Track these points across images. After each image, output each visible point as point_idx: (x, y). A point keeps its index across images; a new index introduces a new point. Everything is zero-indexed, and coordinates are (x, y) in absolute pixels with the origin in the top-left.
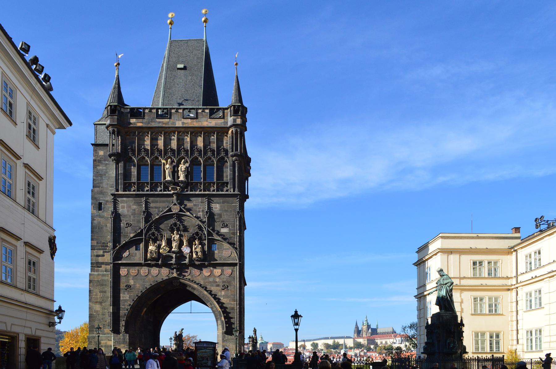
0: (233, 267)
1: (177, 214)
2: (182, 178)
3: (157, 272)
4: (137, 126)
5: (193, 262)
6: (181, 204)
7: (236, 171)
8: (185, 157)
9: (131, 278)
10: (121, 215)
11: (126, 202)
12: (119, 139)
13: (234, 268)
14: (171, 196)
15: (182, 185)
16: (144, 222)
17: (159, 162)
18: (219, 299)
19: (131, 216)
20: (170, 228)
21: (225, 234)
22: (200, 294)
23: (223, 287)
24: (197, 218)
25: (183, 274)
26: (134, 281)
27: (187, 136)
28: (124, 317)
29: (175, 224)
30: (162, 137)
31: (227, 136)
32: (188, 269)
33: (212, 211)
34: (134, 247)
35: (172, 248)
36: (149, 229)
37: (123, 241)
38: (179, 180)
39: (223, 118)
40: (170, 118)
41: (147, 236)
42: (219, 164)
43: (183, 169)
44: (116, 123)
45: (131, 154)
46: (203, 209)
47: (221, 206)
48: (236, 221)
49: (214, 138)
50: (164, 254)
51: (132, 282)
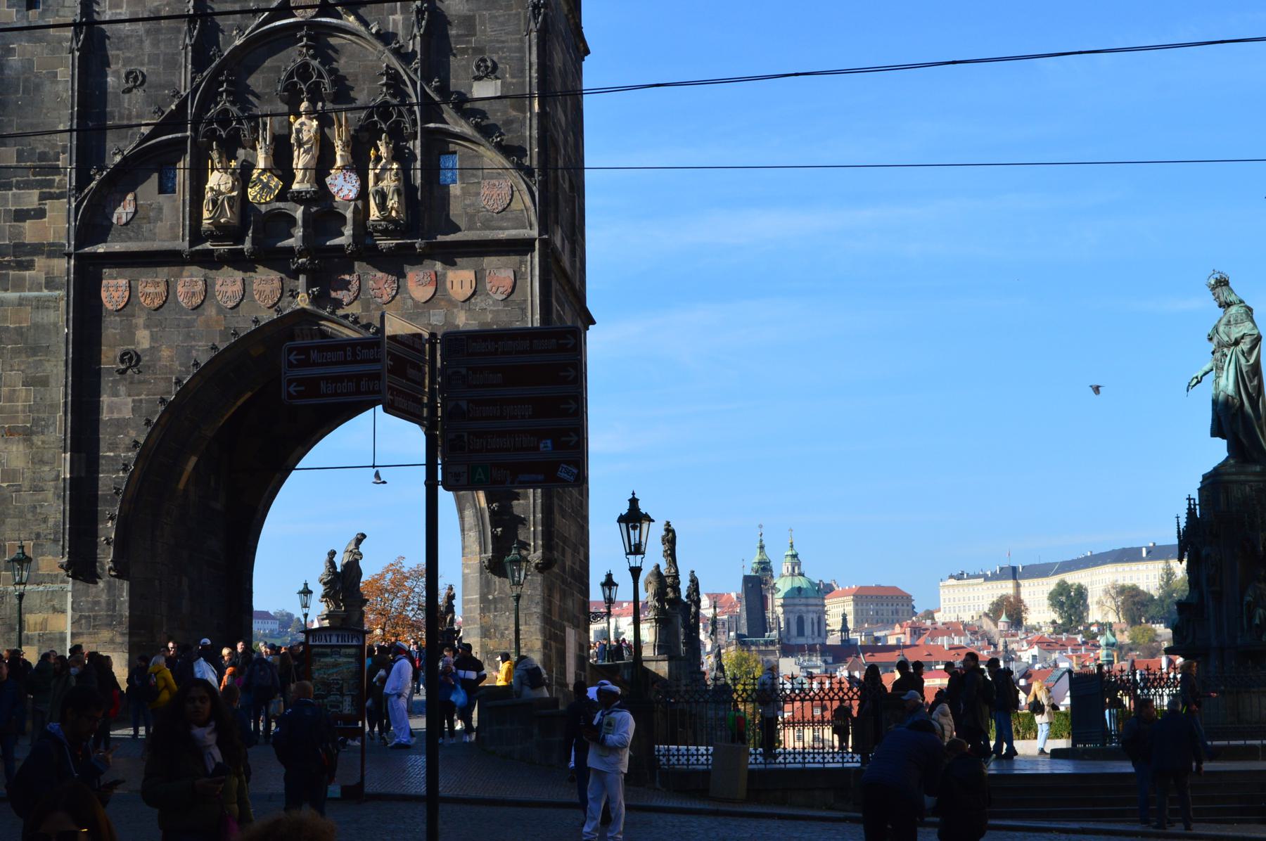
0: (517, 258)
1: (310, 24)
3: (235, 288)
5: (368, 241)
10: (109, 38)
13: (521, 262)
16: (190, 67)
19: (144, 38)
20: (285, 90)
24: (385, 37)
25: (333, 294)
26: (152, 335)
28: (113, 505)
29: (303, 71)
32: (351, 271)
34: (155, 176)
35: (293, 176)
36: (209, 97)
37: (115, 154)
41: (202, 128)
48: (527, 44)
50: (263, 209)
51: (143, 339)
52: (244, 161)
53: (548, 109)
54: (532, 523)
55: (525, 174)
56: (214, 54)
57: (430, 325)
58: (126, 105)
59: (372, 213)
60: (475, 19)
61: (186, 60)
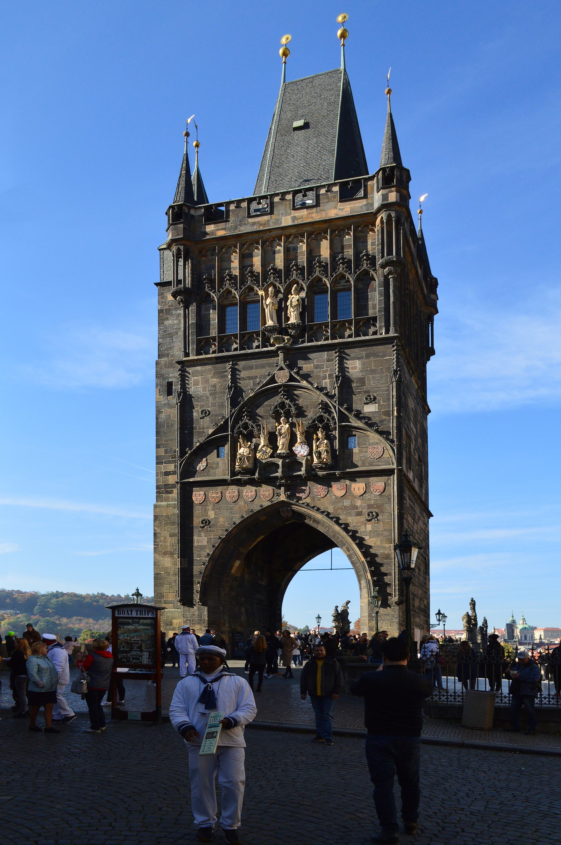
0: (386, 477)
1: (284, 386)
2: (293, 320)
3: (252, 494)
4: (216, 236)
5: (313, 472)
6: (291, 367)
7: (391, 294)
9: (210, 508)
10: (193, 398)
11: (201, 373)
12: (189, 265)
13: (388, 479)
15: (294, 331)
16: (229, 406)
17: (256, 296)
18: (362, 539)
21: (371, 416)
23: (369, 515)
24: (321, 389)
25: (297, 495)
27: (302, 241)
29: (282, 405)
31: (373, 231)
32: (306, 485)
33: (347, 374)
36: (238, 418)
38: (289, 323)
39: (365, 196)
40: (272, 213)
41: (235, 431)
42: (360, 286)
46: (331, 373)
47: (363, 364)
49: (349, 239)
50: (264, 461)
51: (211, 515)
52: (255, 443)
53: (402, 415)
54: (393, 585)
55: (390, 442)
56: (240, 401)
59: (314, 461)
60: (365, 379)
61: (227, 404)
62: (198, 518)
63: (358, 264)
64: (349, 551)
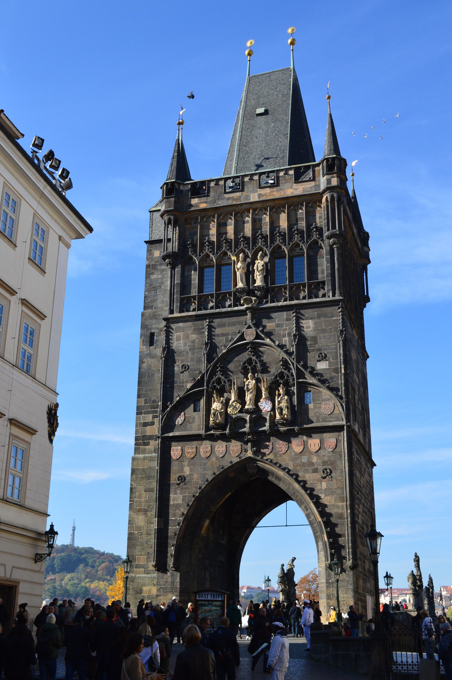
0: (337, 433)
1: (252, 343)
2: (259, 282)
3: (223, 449)
4: (199, 208)
5: (276, 428)
6: (258, 324)
7: (336, 262)
8: (263, 247)
10: (175, 352)
11: (183, 329)
12: (177, 231)
13: (339, 435)
14: (242, 313)
15: (260, 293)
16: (206, 362)
17: (229, 260)
18: (318, 498)
19: (189, 352)
21: (323, 372)
22: (289, 488)
23: (324, 472)
24: (281, 346)
25: (262, 451)
26: (190, 469)
27: (266, 214)
28: (174, 540)
29: (250, 361)
30: (232, 220)
31: (320, 206)
32: (269, 441)
33: (302, 332)
34: (192, 405)
35: (246, 403)
36: (213, 373)
37: (177, 397)
38: (255, 285)
39: (314, 179)
40: (243, 190)
41: (210, 386)
42: (311, 253)
43: (260, 268)
44: (172, 208)
45: (191, 252)
47: (315, 324)
49: (302, 212)
50: (234, 416)
51: (187, 471)
52: (227, 398)
53: (348, 372)
54: (347, 548)
55: (339, 398)
56: (215, 356)
57: (302, 462)
58: (182, 378)
59: (277, 416)
60: (317, 338)
61: (204, 359)
62: (175, 474)
63: (309, 236)
64: (307, 510)
